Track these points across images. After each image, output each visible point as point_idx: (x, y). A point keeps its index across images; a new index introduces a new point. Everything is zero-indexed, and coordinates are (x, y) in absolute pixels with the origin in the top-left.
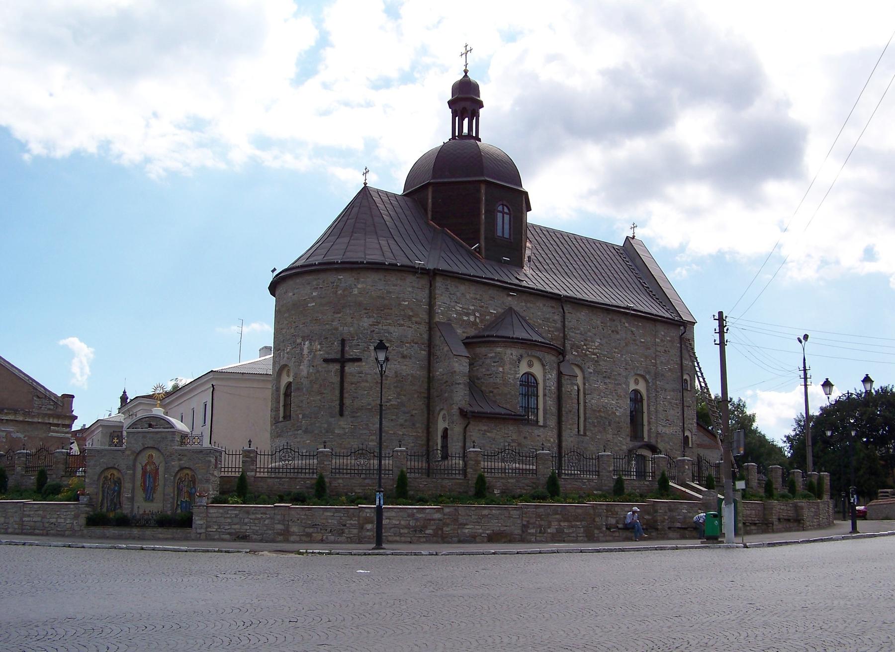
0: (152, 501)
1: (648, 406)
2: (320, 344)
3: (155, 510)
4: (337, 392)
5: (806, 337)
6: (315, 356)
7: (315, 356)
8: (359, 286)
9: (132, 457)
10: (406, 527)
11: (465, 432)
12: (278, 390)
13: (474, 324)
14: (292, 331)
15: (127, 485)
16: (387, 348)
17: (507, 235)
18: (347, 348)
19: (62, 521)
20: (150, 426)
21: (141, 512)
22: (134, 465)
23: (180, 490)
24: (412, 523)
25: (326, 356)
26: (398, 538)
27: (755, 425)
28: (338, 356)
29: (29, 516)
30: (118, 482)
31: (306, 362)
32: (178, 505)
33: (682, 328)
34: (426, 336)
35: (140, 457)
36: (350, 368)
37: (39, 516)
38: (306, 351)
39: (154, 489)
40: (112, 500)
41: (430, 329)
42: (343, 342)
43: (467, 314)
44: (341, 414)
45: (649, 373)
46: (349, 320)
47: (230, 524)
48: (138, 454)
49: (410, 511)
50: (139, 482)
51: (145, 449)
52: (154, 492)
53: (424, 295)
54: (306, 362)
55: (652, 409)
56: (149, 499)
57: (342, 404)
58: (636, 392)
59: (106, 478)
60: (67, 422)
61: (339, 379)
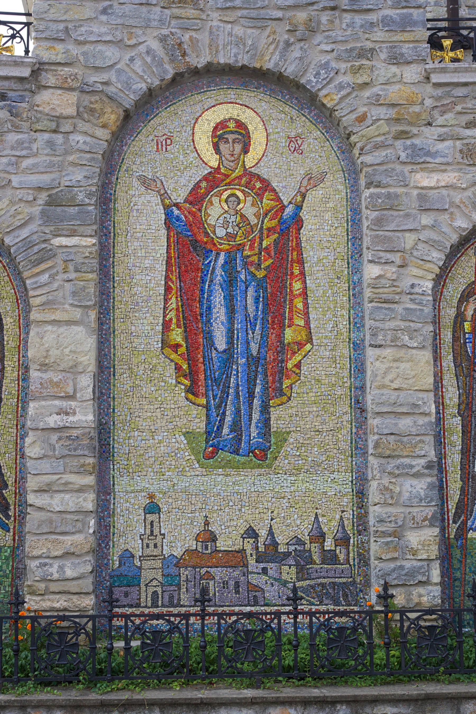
0: (262, 454)
3: (291, 527)
9: (91, 138)
21: (179, 539)
22: (105, 199)
35: (142, 154)
39: (272, 371)
48: (132, 118)
51: (189, 80)
52: (276, 393)
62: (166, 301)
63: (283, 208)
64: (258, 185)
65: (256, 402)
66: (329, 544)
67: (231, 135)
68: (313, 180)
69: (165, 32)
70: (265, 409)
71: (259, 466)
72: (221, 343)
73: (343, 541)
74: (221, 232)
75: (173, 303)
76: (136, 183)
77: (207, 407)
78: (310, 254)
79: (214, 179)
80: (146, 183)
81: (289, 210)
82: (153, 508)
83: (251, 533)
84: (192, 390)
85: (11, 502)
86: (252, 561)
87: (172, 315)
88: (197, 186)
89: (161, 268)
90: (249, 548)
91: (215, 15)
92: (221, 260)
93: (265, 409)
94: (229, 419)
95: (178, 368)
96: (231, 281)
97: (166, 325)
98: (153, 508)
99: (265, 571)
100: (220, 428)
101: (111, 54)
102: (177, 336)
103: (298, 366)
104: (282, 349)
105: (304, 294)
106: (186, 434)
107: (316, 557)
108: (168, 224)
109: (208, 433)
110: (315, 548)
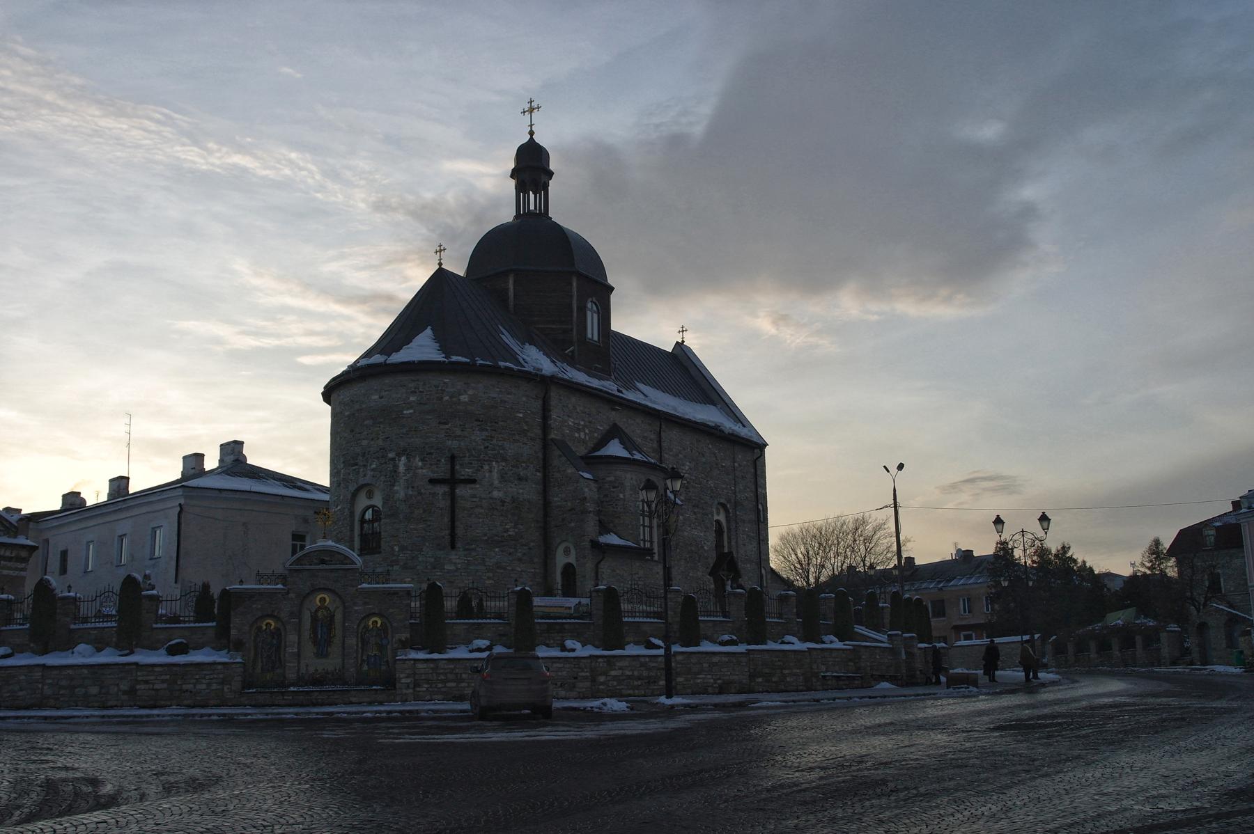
0: (326, 656)
1: (729, 538)
2: (422, 460)
4: (446, 520)
5: (901, 467)
8: (470, 392)
10: (639, 678)
11: (597, 566)
12: (352, 514)
13: (584, 441)
14: (380, 442)
15: (292, 637)
16: (682, 477)
17: (596, 338)
18: (457, 467)
19: (204, 686)
20: (323, 562)
21: (311, 670)
23: (364, 643)
24: (645, 674)
26: (631, 692)
27: (918, 562)
28: (448, 476)
29: (147, 682)
30: (277, 634)
32: (363, 661)
33: (757, 451)
34: (540, 455)
36: (461, 491)
37: (163, 681)
38: (402, 469)
41: (545, 447)
42: (453, 459)
43: (578, 430)
44: (453, 547)
45: (729, 501)
46: (458, 432)
47: (444, 682)
49: (642, 660)
50: (307, 634)
51: (315, 590)
53: (538, 405)
55: (733, 543)
56: (321, 654)
57: (453, 535)
58: (718, 522)
59: (259, 628)
60: (24, 554)
61: (448, 503)
64: (327, 609)
67: (323, 600)
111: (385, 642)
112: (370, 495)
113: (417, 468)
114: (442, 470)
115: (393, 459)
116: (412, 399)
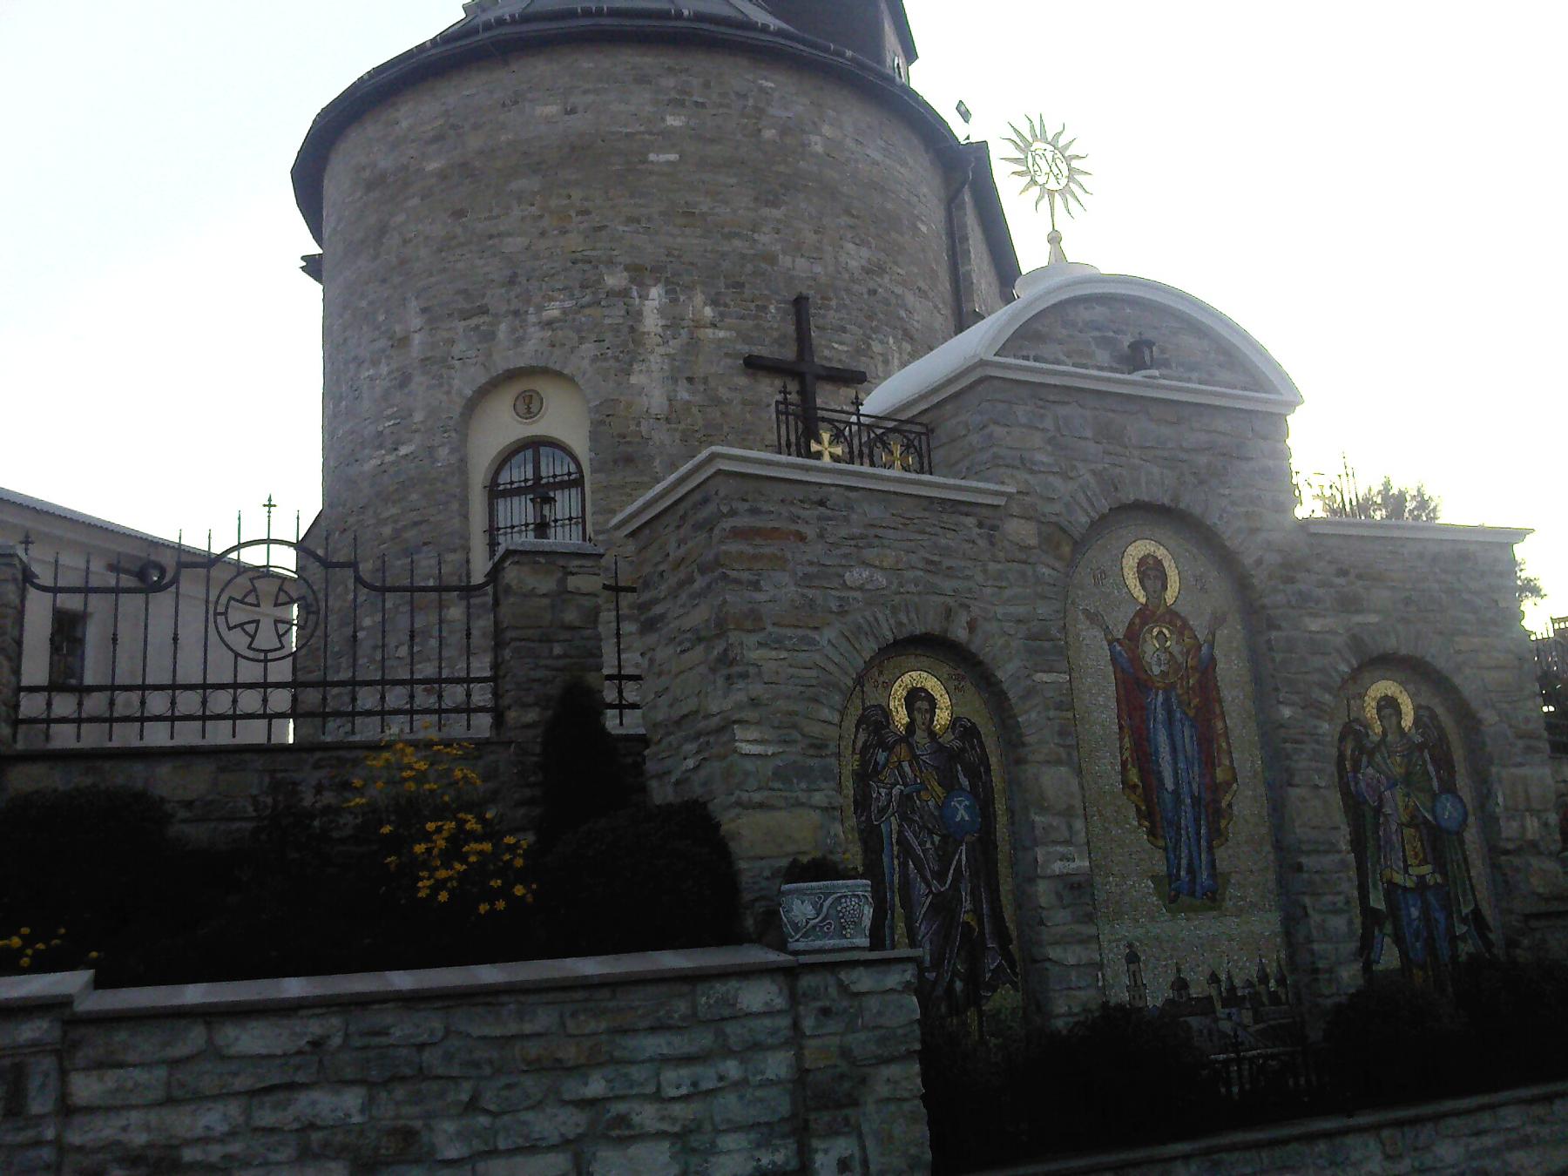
0: (1212, 898)
2: (714, 302)
3: (1243, 970)
6: (693, 345)
7: (693, 345)
25: (745, 349)
31: (656, 361)
32: (1371, 918)
38: (652, 322)
40: (944, 907)
52: (1217, 834)
54: (656, 361)
59: (876, 721)
62: (1121, 739)
63: (1200, 647)
65: (1203, 843)
66: (1272, 983)
68: (1218, 620)
69: (1100, 467)
70: (1210, 849)
71: (1212, 909)
72: (1169, 785)
73: (1281, 981)
74: (1156, 670)
75: (1127, 743)
76: (1081, 617)
77: (1165, 849)
78: (1228, 694)
79: (1145, 615)
80: (1093, 618)
81: (1204, 649)
82: (1132, 958)
83: (1214, 978)
84: (1152, 833)
85: (1017, 957)
86: (1218, 1007)
87: (1127, 754)
88: (1131, 624)
89: (1113, 705)
90: (1214, 993)
91: (1136, 453)
92: (1160, 698)
93: (1210, 849)
94: (1184, 862)
95: (1138, 809)
96: (1170, 722)
97: (1124, 764)
98: (1132, 958)
99: (1229, 1016)
100: (1179, 871)
101: (1057, 482)
102: (1134, 776)
103: (1230, 805)
104: (1216, 789)
105: (1226, 735)
106: (1153, 878)
107: (1265, 999)
108: (1114, 660)
109: (1170, 875)
110: (1262, 988)
111: (1448, 810)
112: (529, 406)
113: (698, 324)
114: (775, 342)
115: (624, 293)
116: (673, 121)
